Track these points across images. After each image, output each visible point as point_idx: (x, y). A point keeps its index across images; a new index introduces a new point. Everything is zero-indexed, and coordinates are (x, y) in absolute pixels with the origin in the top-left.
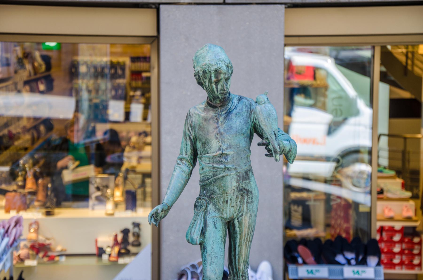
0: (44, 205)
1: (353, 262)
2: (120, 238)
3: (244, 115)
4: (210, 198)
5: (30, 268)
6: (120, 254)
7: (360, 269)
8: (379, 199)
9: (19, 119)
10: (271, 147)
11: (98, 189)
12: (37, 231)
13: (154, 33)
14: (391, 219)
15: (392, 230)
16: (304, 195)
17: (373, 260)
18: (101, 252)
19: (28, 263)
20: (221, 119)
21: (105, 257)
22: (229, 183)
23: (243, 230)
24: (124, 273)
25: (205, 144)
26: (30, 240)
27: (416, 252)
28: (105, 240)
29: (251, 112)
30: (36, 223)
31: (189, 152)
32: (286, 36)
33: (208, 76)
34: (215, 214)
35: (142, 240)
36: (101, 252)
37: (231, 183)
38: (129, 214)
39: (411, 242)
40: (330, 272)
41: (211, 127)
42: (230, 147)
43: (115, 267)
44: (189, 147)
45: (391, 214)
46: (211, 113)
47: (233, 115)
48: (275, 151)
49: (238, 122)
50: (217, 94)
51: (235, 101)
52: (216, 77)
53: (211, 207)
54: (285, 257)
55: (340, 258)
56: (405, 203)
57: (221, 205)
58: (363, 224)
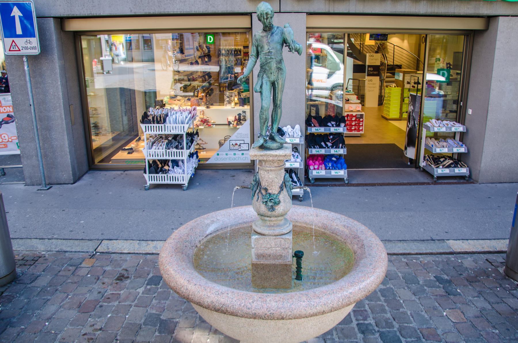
0: (206, 104)
1: (334, 125)
2: (237, 118)
3: (279, 34)
4: (264, 72)
5: (201, 129)
6: (237, 124)
7: (337, 128)
8: (346, 103)
9: (197, 72)
10: (291, 47)
11: (228, 97)
12: (203, 114)
13: (250, 27)
14: (352, 111)
15: (352, 116)
16: (317, 102)
17: (343, 125)
18: (229, 123)
19: (200, 127)
20: (269, 36)
21: (231, 125)
22: (272, 65)
23: (279, 86)
24: (238, 131)
25: (262, 47)
26: (201, 118)
27: (361, 124)
28: (231, 118)
29: (282, 33)
30: (203, 111)
31: (255, 52)
32: (307, 28)
33: (263, 16)
34: (267, 79)
35: (246, 118)
36: (229, 123)
37: (274, 65)
38: (241, 107)
39: (359, 120)
40: (325, 130)
41: (265, 40)
42: (273, 48)
43: (235, 129)
44: (255, 50)
45: (352, 109)
46: (265, 34)
47: (274, 35)
48: (292, 49)
49: (277, 38)
50: (267, 24)
51: (275, 29)
52: (267, 16)
53: (265, 76)
54: (306, 123)
55: (329, 124)
56: (358, 105)
57: (269, 75)
58: (339, 111)
